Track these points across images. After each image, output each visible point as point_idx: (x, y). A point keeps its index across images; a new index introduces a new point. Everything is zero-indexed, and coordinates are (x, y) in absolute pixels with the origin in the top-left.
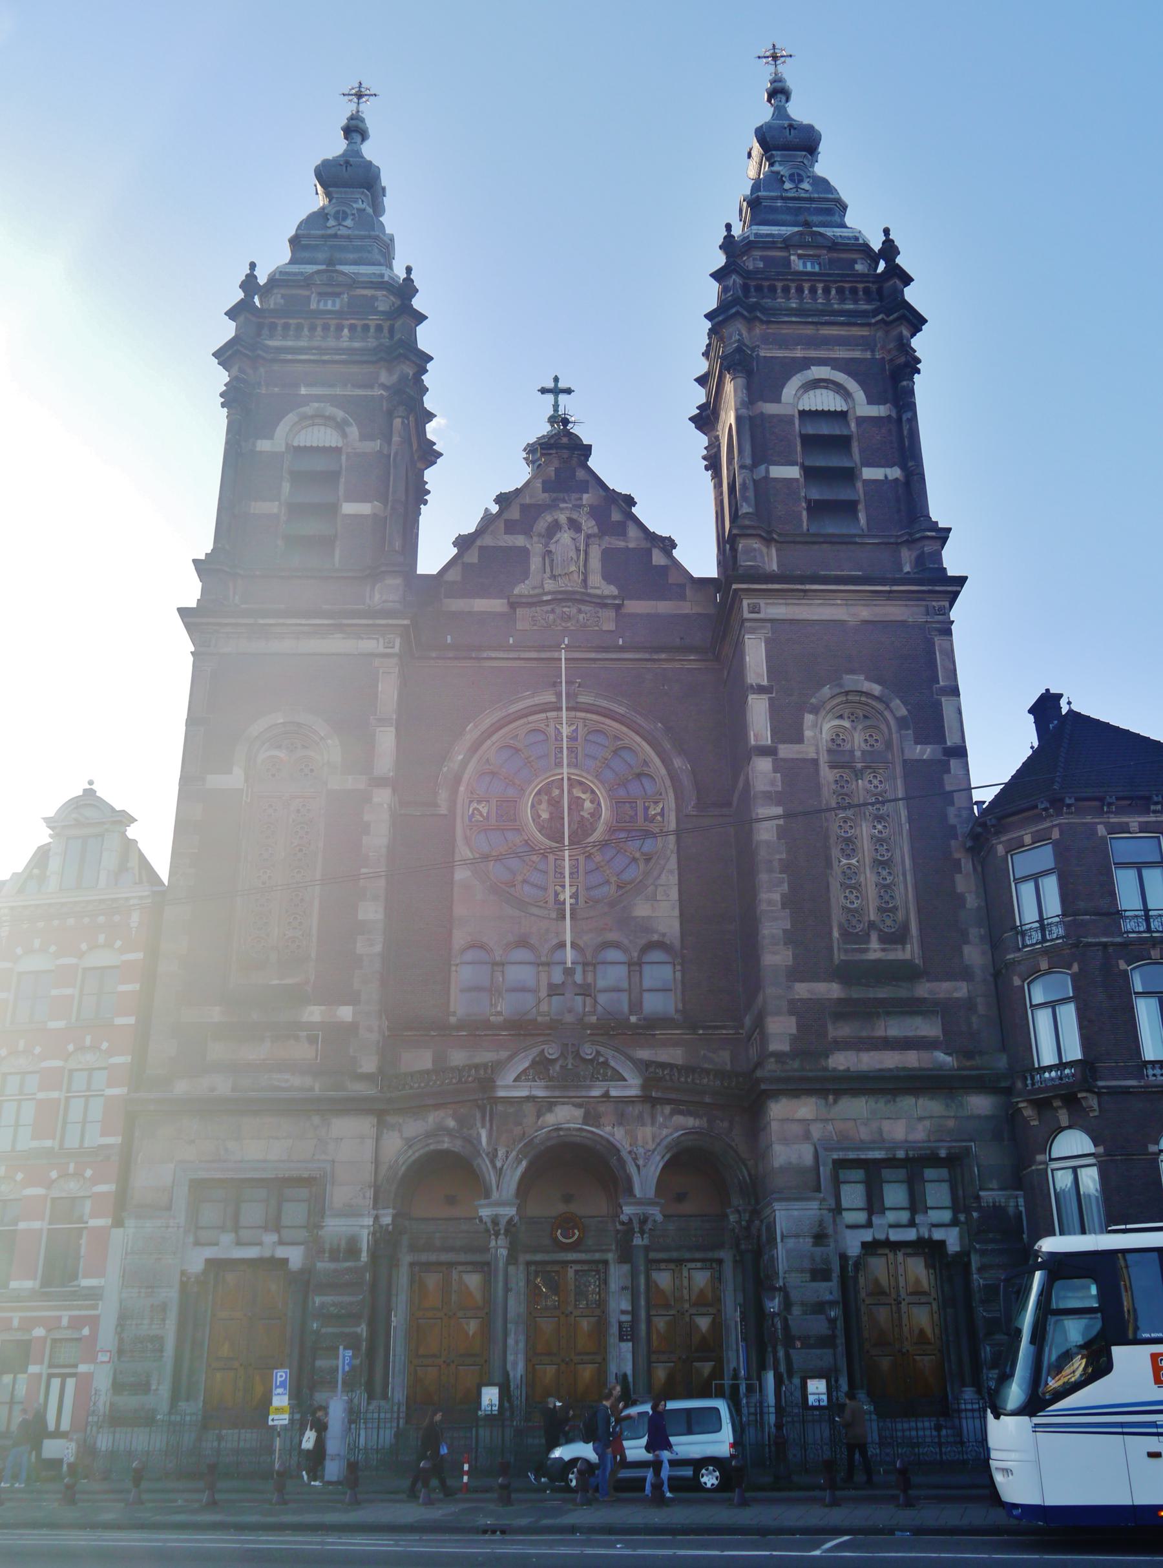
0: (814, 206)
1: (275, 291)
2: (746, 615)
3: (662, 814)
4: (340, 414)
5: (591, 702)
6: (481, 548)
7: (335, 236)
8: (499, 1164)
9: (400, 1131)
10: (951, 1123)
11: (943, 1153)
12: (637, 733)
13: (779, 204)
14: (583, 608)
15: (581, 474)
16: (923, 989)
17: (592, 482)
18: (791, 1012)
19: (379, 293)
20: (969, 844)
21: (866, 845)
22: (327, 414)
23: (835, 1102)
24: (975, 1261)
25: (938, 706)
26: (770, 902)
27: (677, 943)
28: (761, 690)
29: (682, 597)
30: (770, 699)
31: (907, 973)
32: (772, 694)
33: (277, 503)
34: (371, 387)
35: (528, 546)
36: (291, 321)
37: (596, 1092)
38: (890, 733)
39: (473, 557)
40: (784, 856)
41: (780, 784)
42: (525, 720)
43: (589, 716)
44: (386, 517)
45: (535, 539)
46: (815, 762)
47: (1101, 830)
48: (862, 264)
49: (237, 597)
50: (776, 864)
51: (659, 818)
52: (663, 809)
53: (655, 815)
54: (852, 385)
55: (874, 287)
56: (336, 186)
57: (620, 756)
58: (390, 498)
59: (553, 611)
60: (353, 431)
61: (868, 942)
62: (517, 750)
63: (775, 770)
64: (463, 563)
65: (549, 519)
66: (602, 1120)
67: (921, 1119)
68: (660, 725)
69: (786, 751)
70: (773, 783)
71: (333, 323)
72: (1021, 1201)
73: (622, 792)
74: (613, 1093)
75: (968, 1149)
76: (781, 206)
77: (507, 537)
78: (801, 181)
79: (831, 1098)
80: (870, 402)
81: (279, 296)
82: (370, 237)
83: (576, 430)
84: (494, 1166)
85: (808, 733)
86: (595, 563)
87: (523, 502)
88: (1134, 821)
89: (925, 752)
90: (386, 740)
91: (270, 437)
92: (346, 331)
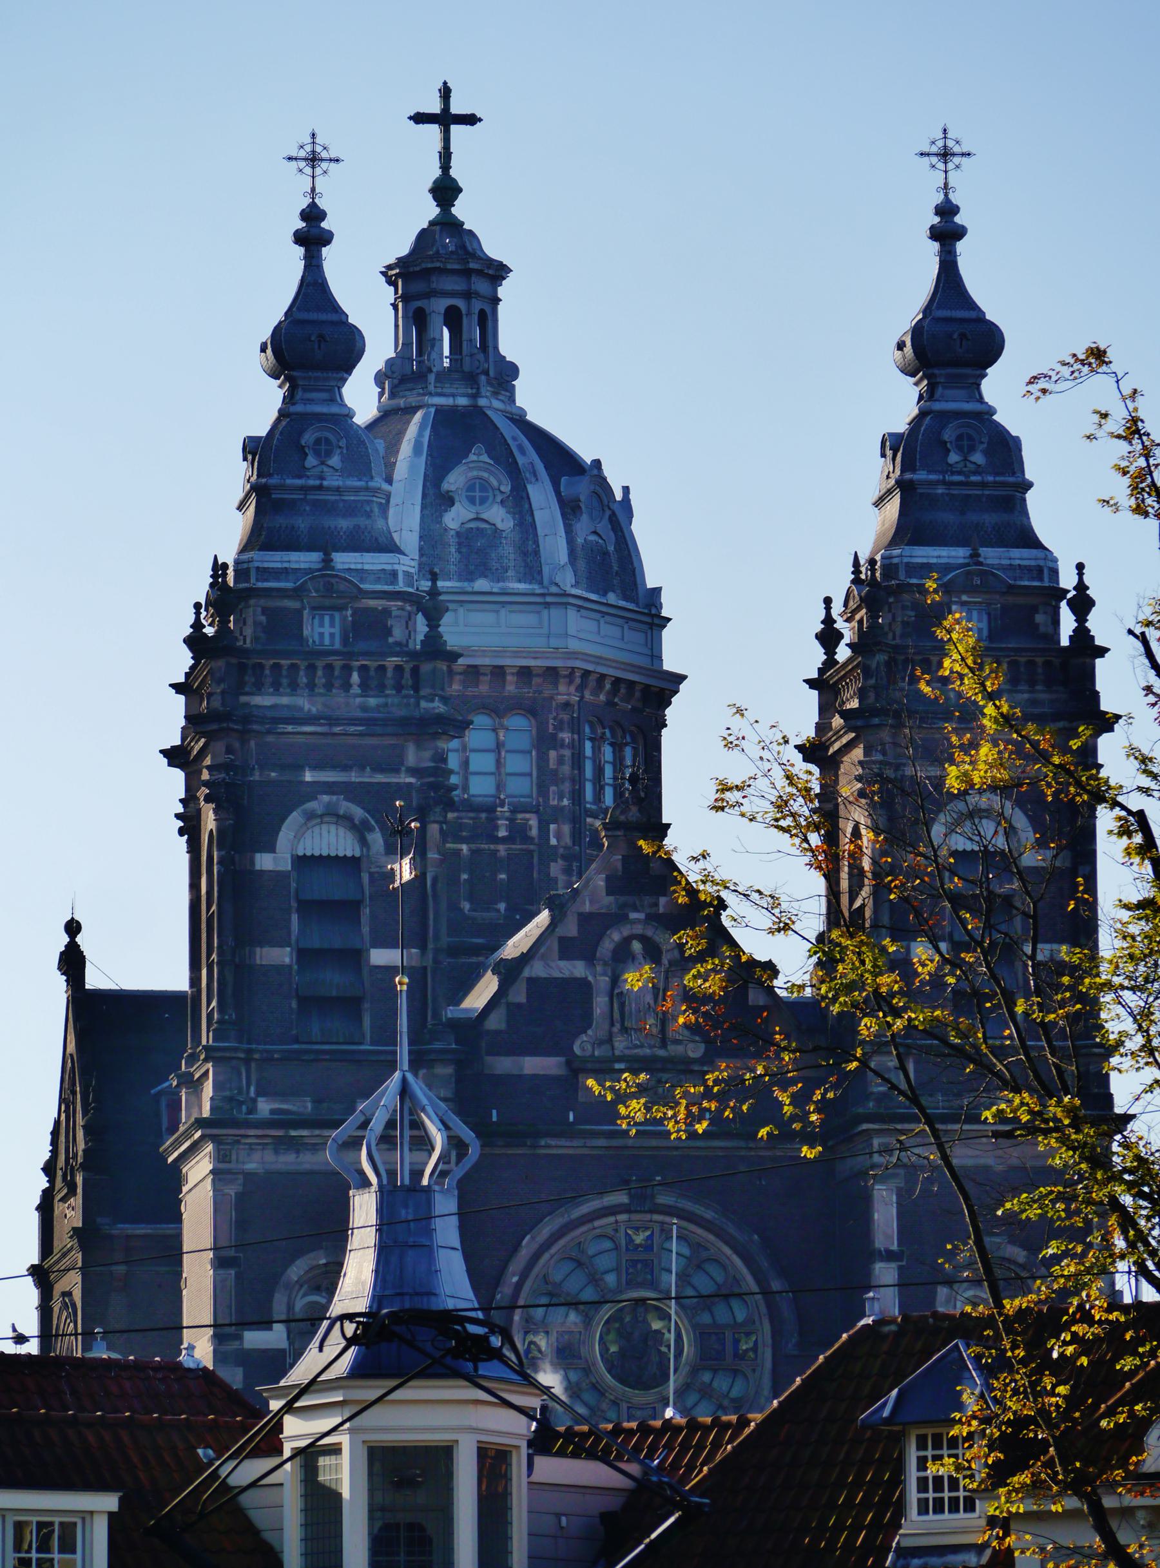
0: (987, 492)
1: (252, 602)
3: (755, 1349)
4: (358, 812)
5: (671, 1203)
6: (531, 981)
7: (320, 488)
12: (727, 1243)
13: (940, 491)
19: (394, 605)
22: (341, 812)
28: (890, 1256)
30: (900, 1268)
32: (902, 1261)
33: (288, 949)
34: (397, 771)
35: (590, 978)
36: (283, 662)
39: (519, 995)
42: (590, 1226)
44: (425, 968)
45: (599, 969)
48: (1045, 613)
49: (252, 1089)
51: (751, 1354)
52: (756, 1342)
53: (747, 1351)
54: (1020, 821)
57: (707, 1273)
58: (431, 946)
60: (376, 839)
62: (580, 1264)
64: (508, 1005)
65: (616, 937)
68: (756, 1237)
71: (338, 664)
73: (706, 1318)
76: (942, 494)
77: (562, 963)
78: (972, 449)
80: (1041, 844)
81: (259, 609)
82: (367, 489)
87: (581, 910)
91: (272, 849)
92: (355, 678)
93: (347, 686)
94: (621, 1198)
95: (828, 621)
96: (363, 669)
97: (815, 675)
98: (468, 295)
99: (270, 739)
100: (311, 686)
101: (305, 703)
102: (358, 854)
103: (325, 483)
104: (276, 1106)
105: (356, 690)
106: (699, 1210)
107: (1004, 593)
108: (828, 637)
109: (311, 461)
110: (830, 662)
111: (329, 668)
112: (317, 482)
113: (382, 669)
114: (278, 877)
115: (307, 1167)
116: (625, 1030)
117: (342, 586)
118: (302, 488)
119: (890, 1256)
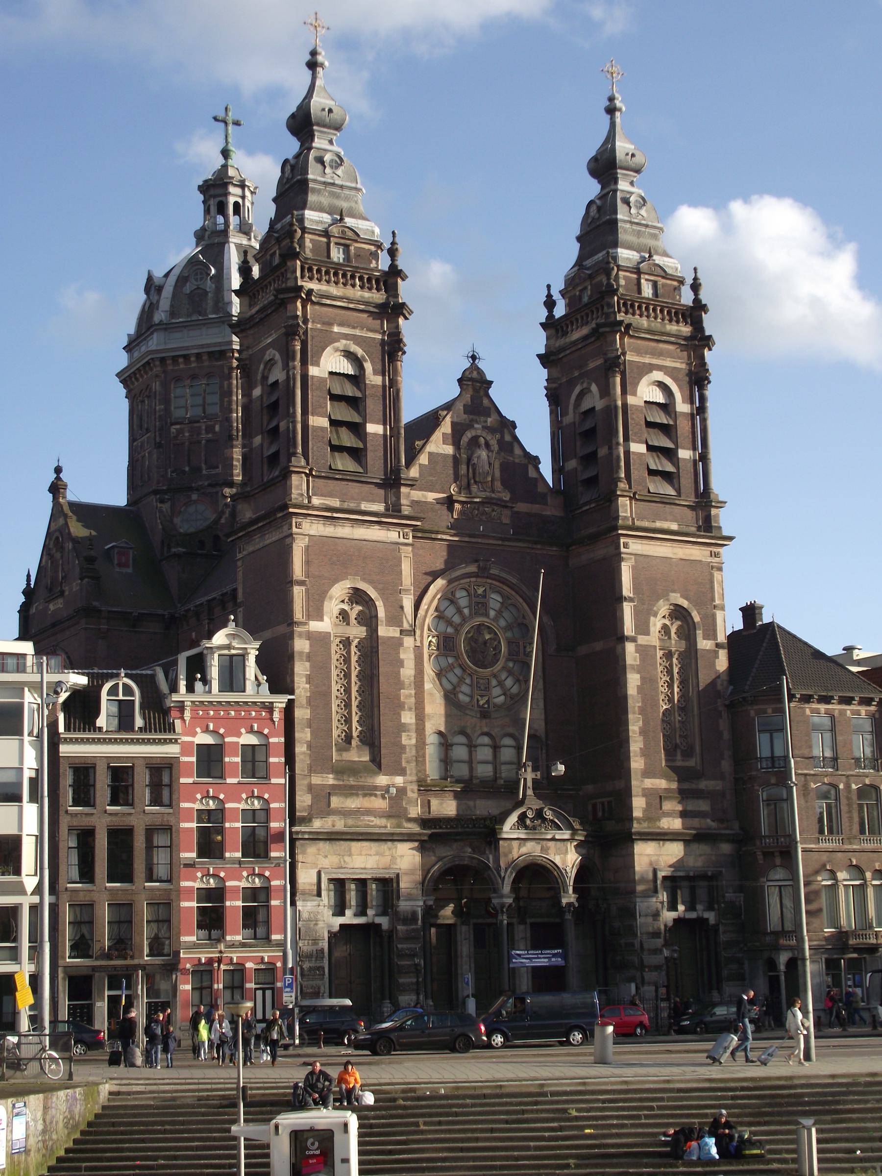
2: (623, 550)
6: (430, 454)
7: (333, 184)
8: (503, 874)
9: (434, 852)
10: (713, 858)
11: (710, 874)
12: (521, 596)
14: (496, 508)
15: (486, 402)
16: (703, 785)
17: (493, 409)
18: (644, 795)
20: (727, 702)
24: (721, 929)
25: (714, 618)
26: (634, 732)
27: (543, 736)
29: (546, 504)
37: (549, 837)
38: (689, 631)
40: (640, 704)
43: (494, 582)
47: (808, 712)
50: (637, 709)
55: (688, 313)
56: (318, 125)
59: (478, 510)
61: (675, 755)
66: (550, 851)
67: (700, 855)
69: (642, 640)
70: (635, 660)
72: (742, 899)
74: (557, 837)
75: (721, 872)
77: (445, 446)
83: (481, 365)
84: (500, 876)
85: (652, 629)
86: (497, 473)
88: (823, 707)
90: (408, 603)
91: (318, 365)
93: (353, 286)
94: (473, 568)
95: (549, 296)
96: (361, 279)
97: (544, 321)
99: (317, 307)
100: (336, 283)
101: (334, 290)
102: (358, 374)
103: (337, 182)
104: (322, 501)
105: (358, 288)
106: (509, 577)
107: (663, 277)
108: (550, 304)
109: (328, 170)
110: (550, 316)
111: (344, 276)
112: (332, 181)
113: (369, 280)
114: (322, 380)
115: (339, 535)
116: (476, 482)
117: (350, 234)
118: (325, 183)
119: (631, 600)
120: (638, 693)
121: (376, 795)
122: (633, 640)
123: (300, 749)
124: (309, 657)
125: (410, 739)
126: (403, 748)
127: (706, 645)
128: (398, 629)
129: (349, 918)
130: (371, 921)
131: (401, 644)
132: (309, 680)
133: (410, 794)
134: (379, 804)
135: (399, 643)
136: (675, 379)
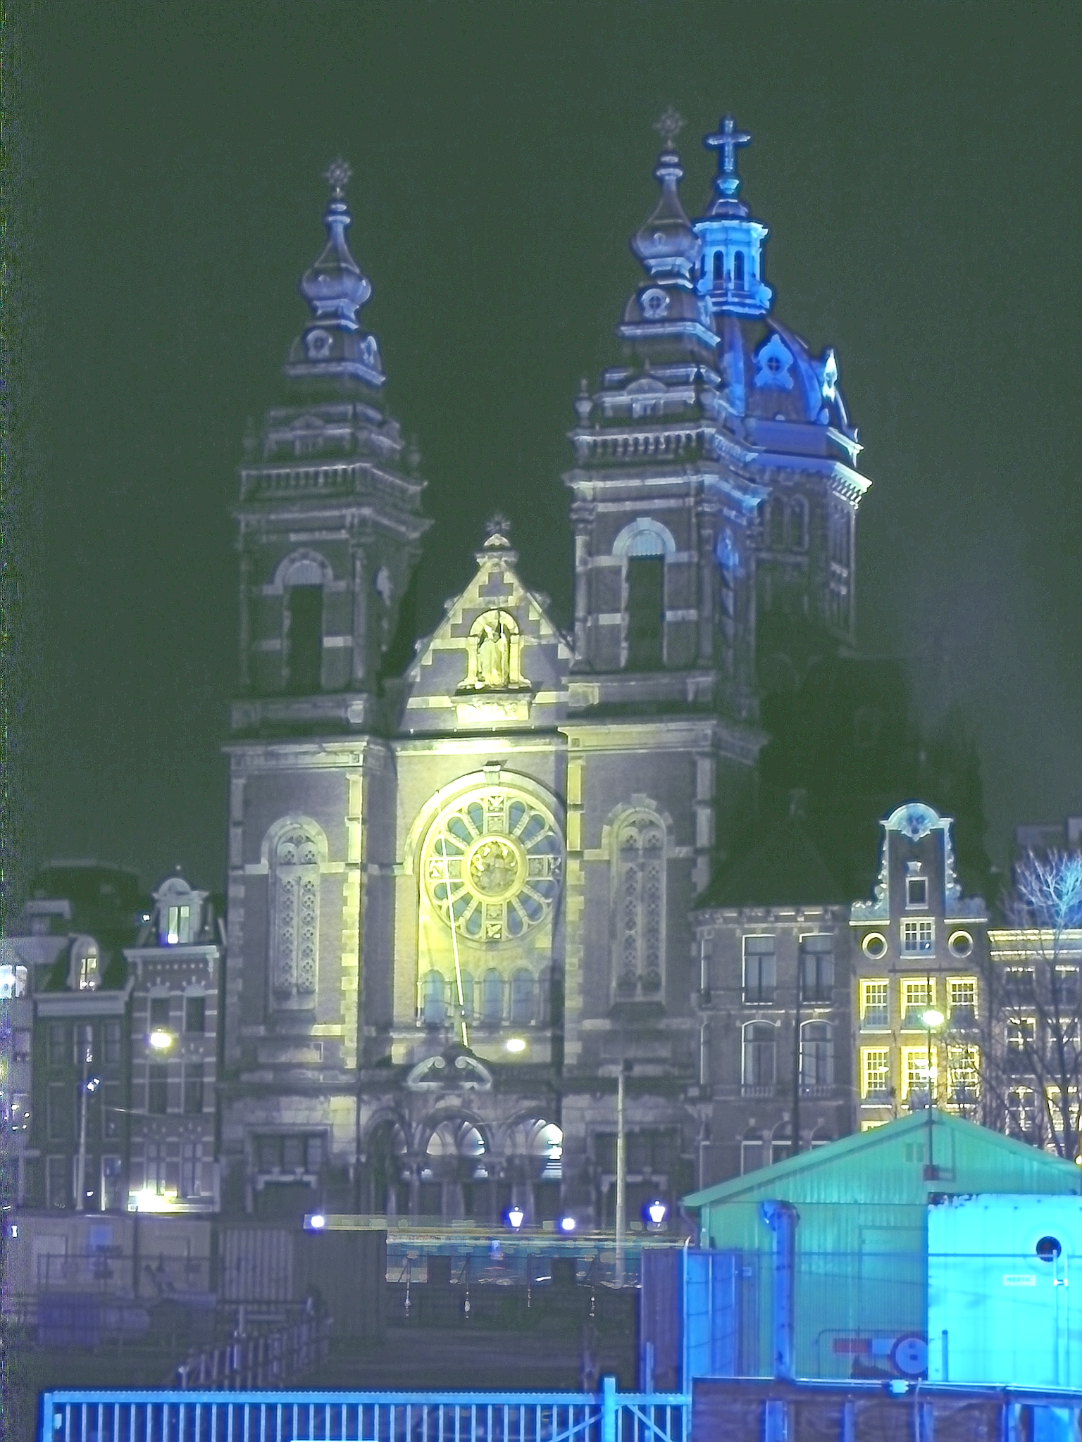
4: (319, 557)
21: (640, 920)
23: (601, 1098)
28: (576, 807)
30: (581, 814)
31: (659, 1011)
40: (581, 932)
41: (583, 879)
46: (608, 862)
50: (577, 938)
60: (330, 572)
63: (581, 870)
64: (424, 667)
69: (589, 855)
70: (579, 879)
79: (598, 1095)
85: (604, 841)
89: (683, 852)
98: (726, 242)
119: (576, 807)
120: (580, 919)
121: (308, 1046)
122: (577, 854)
123: (232, 1000)
124: (244, 903)
125: (351, 984)
126: (343, 993)
127: (680, 852)
128: (343, 864)
129: (276, 1176)
130: (298, 1177)
131: (346, 880)
132: (243, 926)
133: (347, 1043)
134: (313, 1056)
135: (343, 879)
136: (666, 523)
